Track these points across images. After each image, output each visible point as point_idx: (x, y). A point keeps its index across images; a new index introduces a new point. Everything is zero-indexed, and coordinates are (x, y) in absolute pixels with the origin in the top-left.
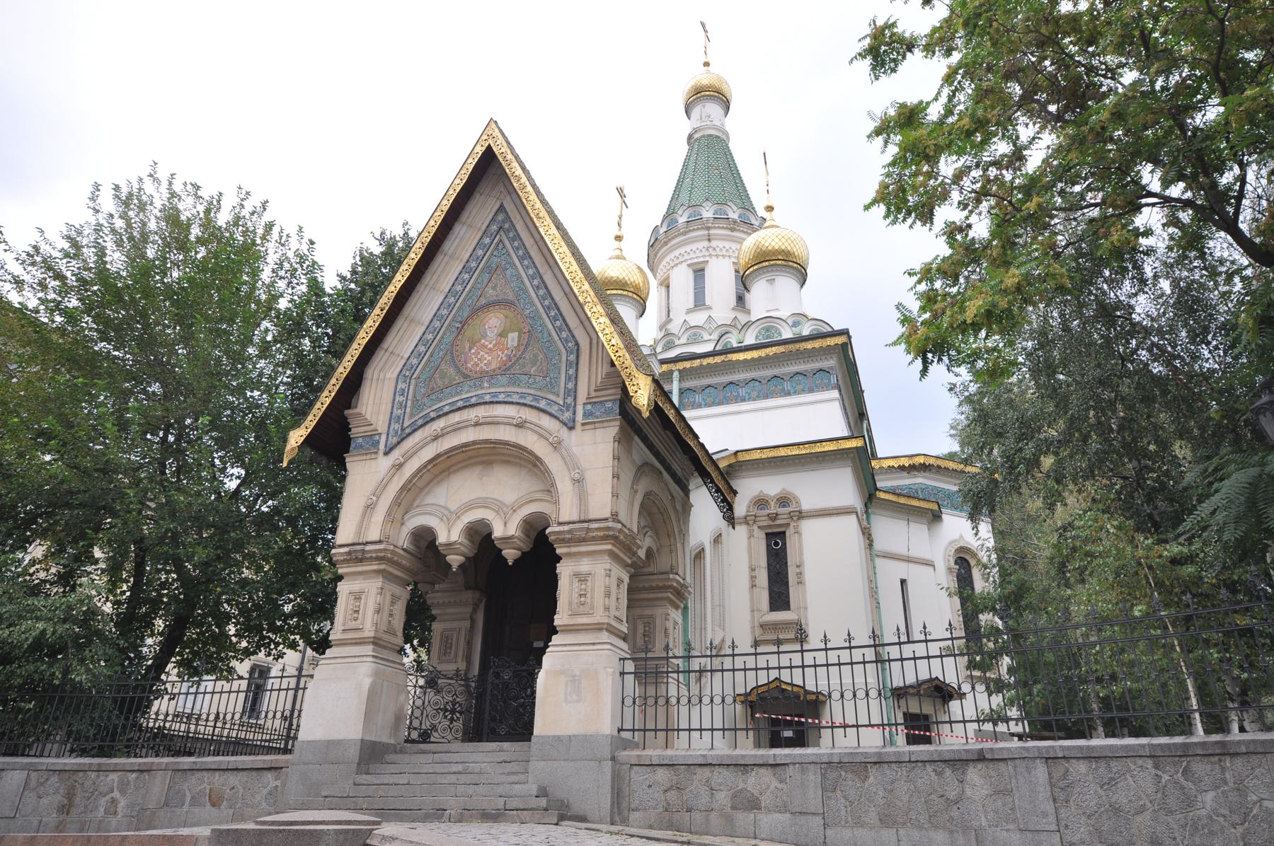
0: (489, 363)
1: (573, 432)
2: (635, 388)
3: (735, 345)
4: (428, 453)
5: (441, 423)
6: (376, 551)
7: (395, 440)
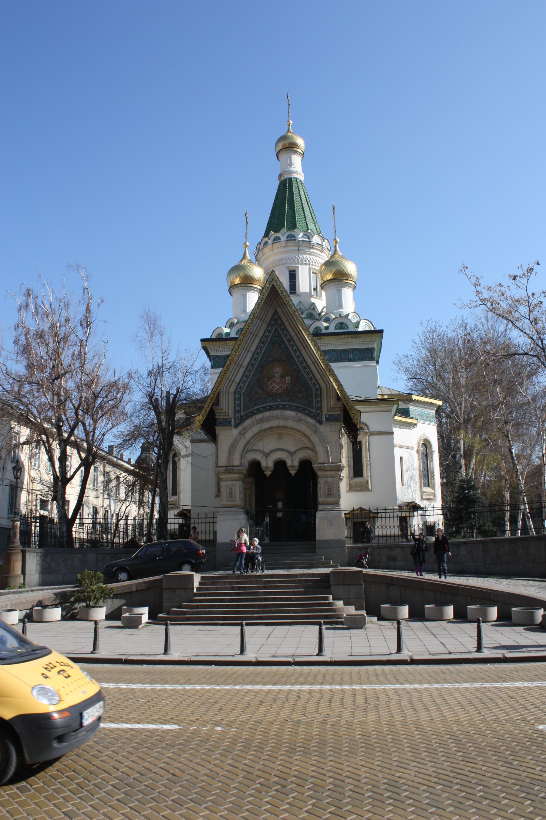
0: (278, 390)
1: (322, 426)
2: (353, 415)
3: (324, 331)
5: (260, 416)
6: (238, 470)
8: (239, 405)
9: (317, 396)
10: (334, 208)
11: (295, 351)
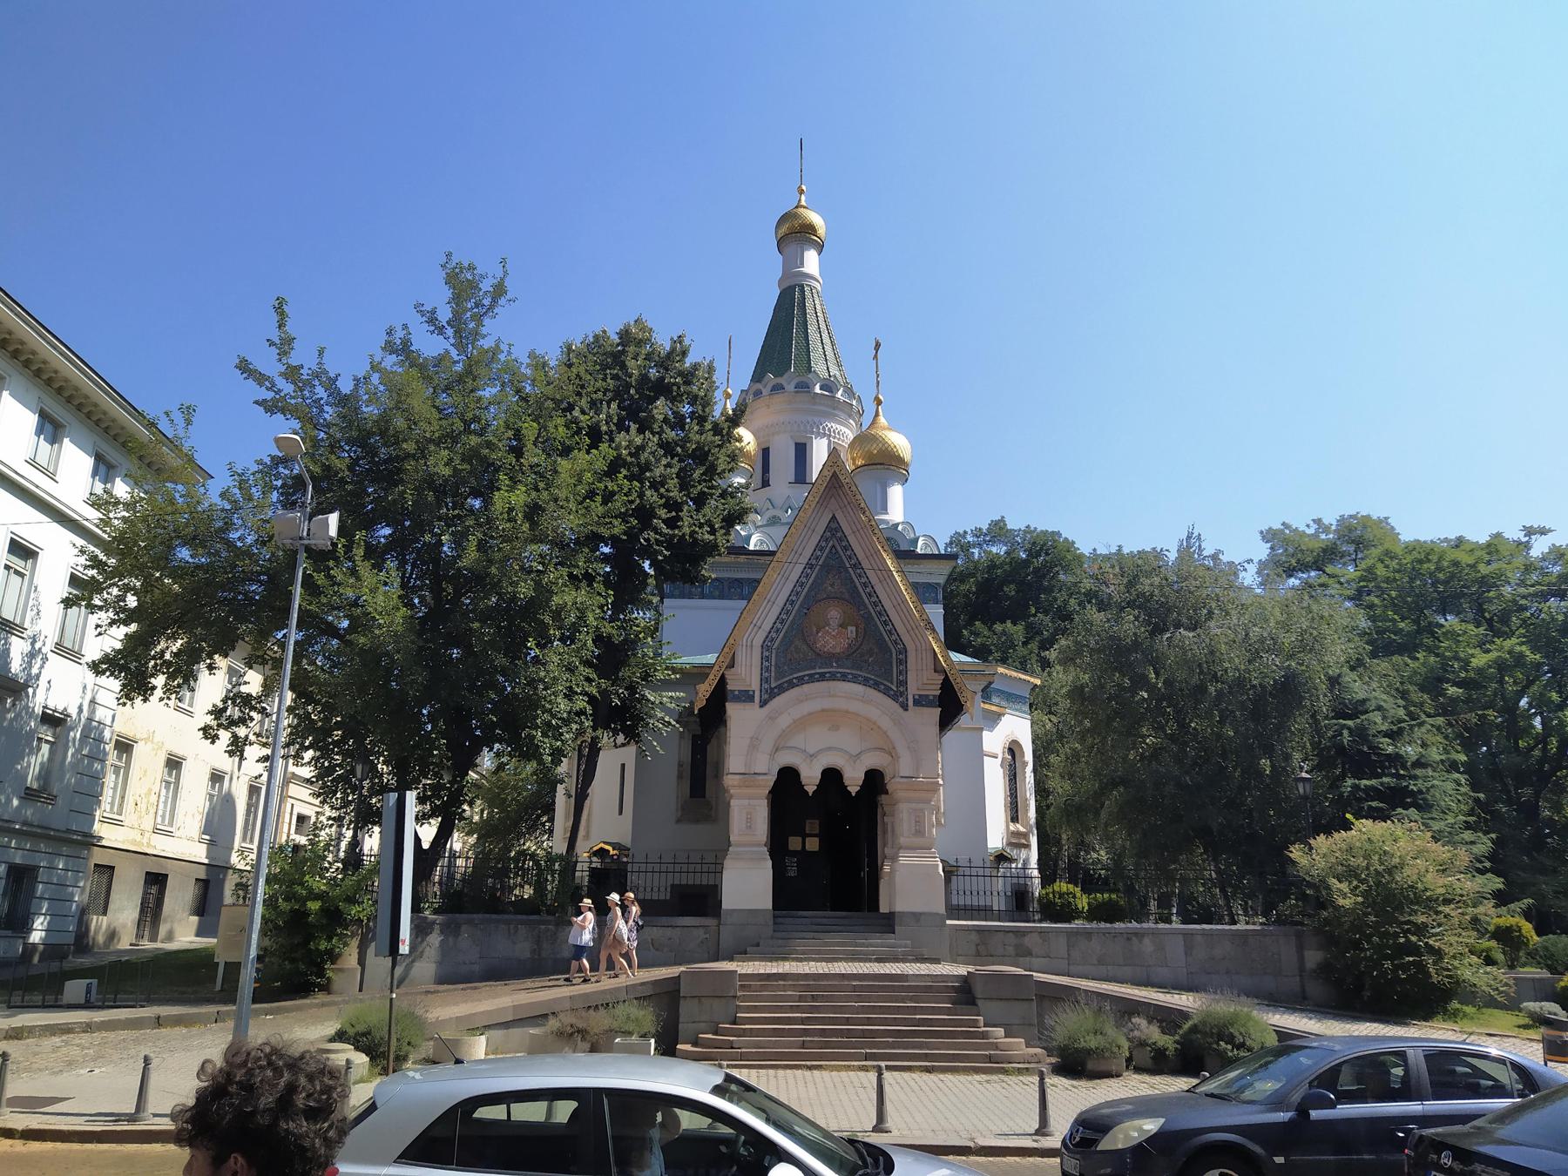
0: (834, 647)
8: (768, 670)
9: (900, 662)
10: (878, 346)
11: (865, 585)
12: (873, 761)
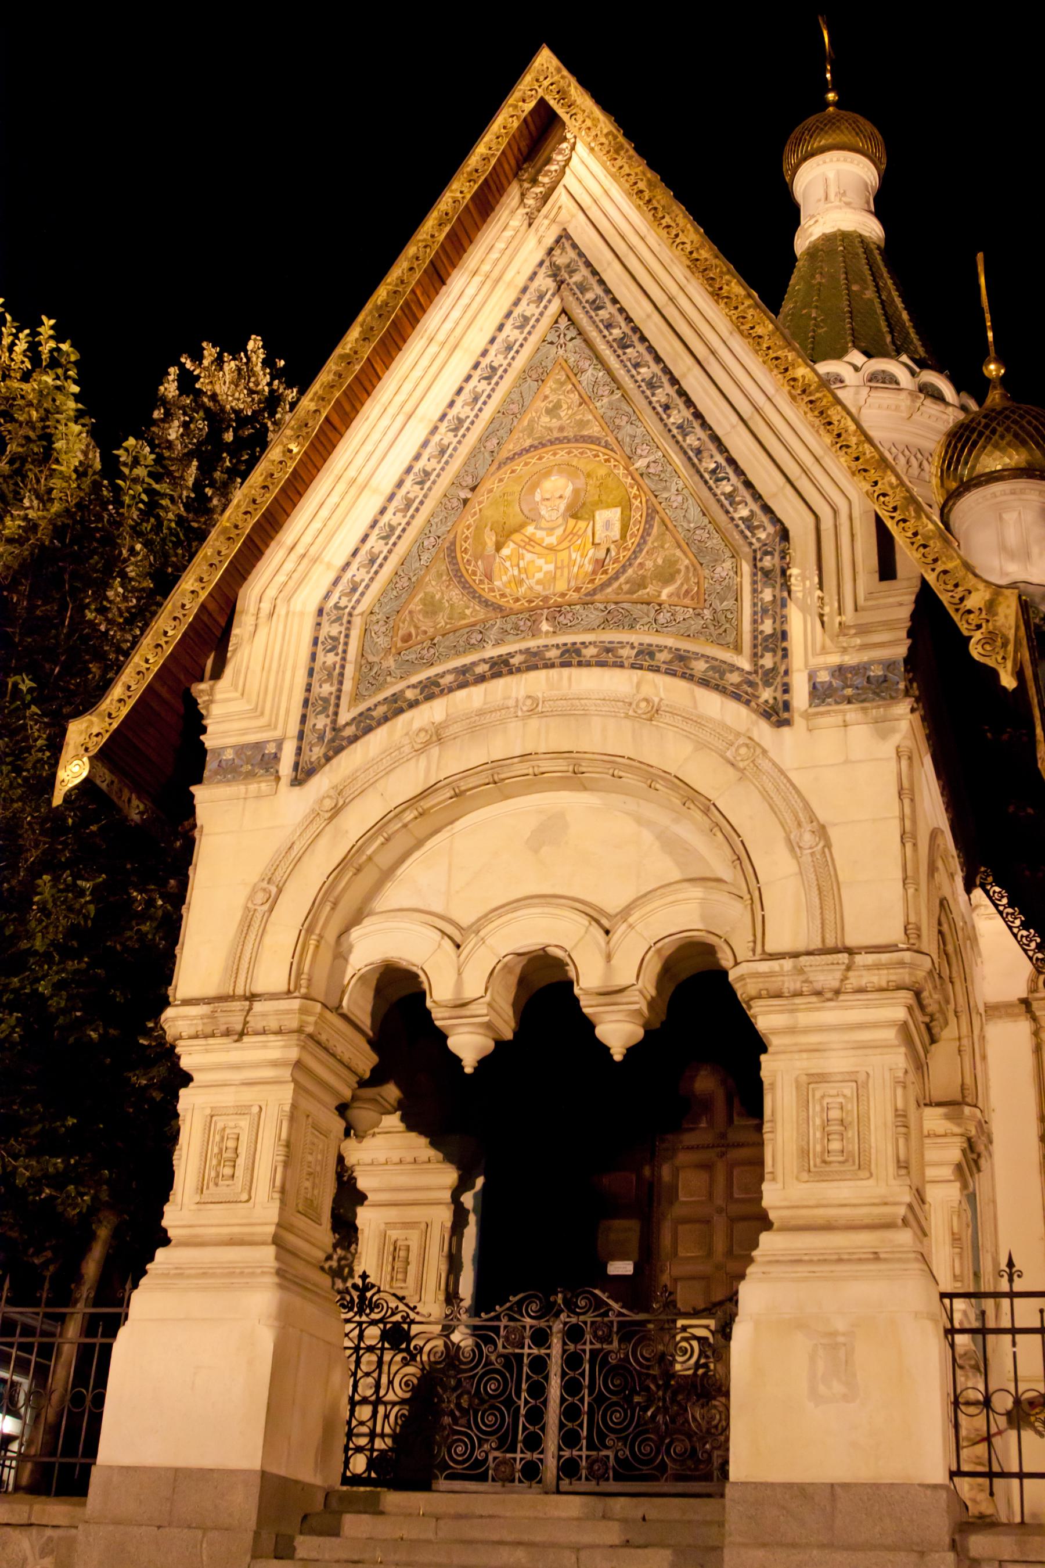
4: (404, 784)
7: (318, 752)
12: (681, 916)
